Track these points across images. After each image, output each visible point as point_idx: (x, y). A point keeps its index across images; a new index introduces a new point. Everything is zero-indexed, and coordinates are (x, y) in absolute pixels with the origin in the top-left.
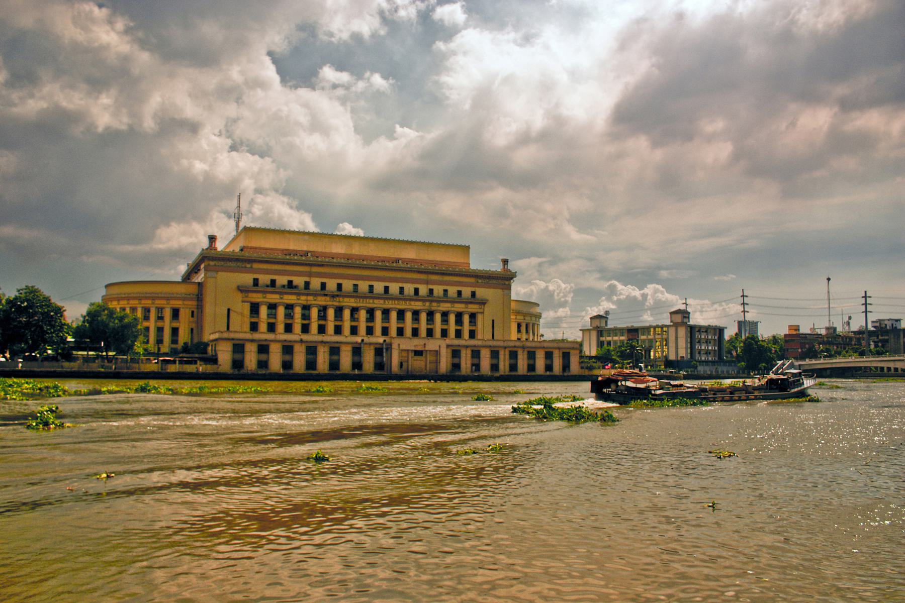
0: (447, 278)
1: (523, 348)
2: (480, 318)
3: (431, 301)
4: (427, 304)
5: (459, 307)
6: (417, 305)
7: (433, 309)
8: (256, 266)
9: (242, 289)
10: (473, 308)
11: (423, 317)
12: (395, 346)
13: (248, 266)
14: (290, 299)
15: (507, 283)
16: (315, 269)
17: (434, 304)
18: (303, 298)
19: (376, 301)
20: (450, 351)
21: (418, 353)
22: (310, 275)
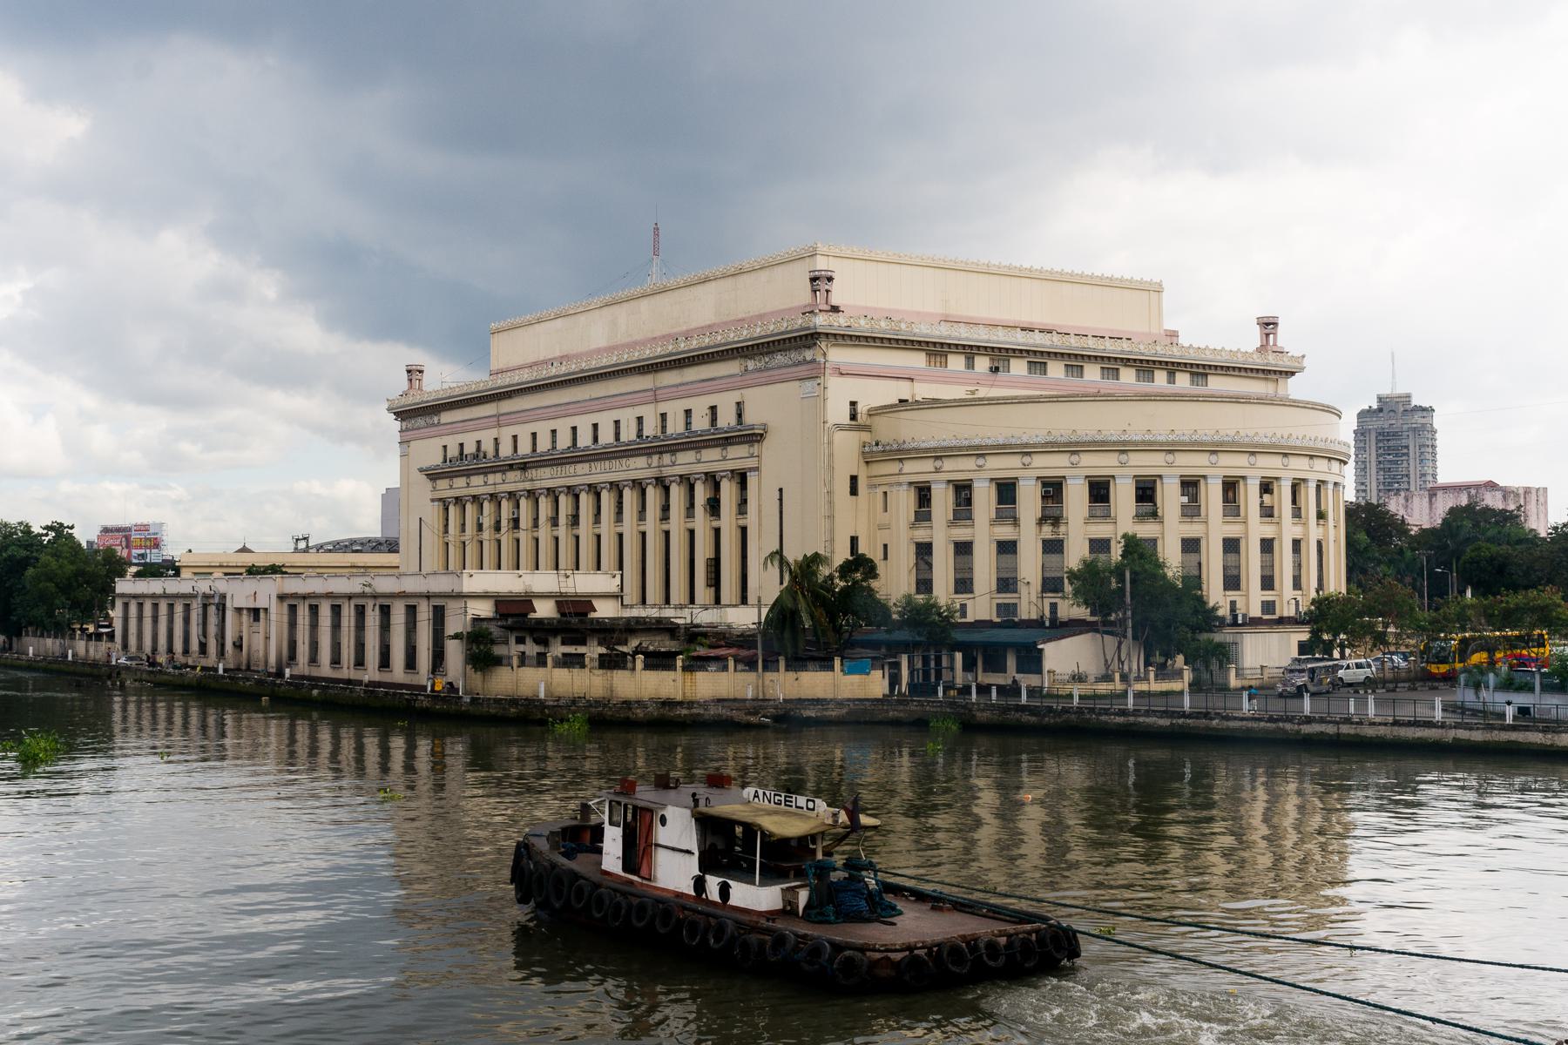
0: (692, 374)
1: (375, 596)
2: (752, 480)
3: (660, 451)
4: (655, 458)
5: (712, 459)
6: (638, 467)
7: (667, 471)
8: (446, 417)
9: (433, 475)
10: (737, 456)
11: (653, 494)
12: (228, 604)
13: (436, 419)
14: (478, 485)
15: (808, 354)
16: (506, 406)
17: (667, 458)
18: (491, 478)
19: (582, 468)
20: (285, 605)
21: (255, 613)
22: (499, 421)
